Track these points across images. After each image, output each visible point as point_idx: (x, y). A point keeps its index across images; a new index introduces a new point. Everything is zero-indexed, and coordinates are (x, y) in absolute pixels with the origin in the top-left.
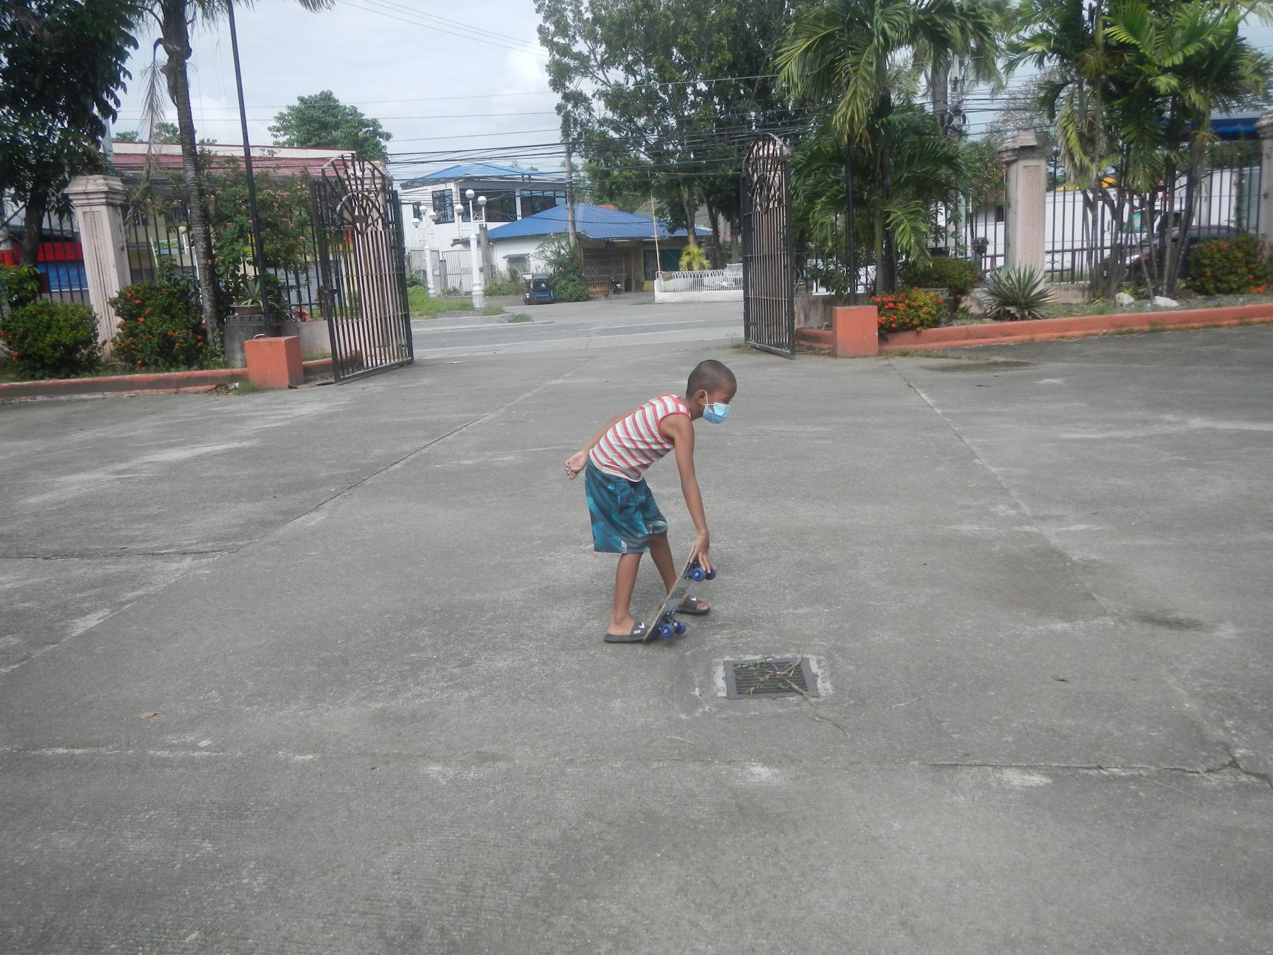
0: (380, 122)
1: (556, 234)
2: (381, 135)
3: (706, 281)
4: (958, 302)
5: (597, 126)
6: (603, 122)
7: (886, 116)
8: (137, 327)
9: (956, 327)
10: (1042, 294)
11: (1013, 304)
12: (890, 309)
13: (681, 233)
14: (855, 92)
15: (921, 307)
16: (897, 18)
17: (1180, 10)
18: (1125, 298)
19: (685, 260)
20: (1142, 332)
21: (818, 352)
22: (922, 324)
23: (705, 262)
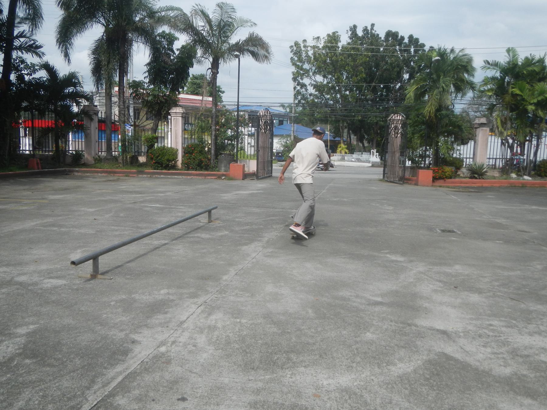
0: (221, 87)
1: (286, 135)
2: (221, 92)
3: (346, 158)
4: (457, 172)
5: (309, 96)
6: (311, 95)
7: (441, 112)
8: (191, 156)
9: (457, 180)
10: (486, 172)
11: (476, 174)
12: (436, 172)
13: (337, 139)
14: (431, 104)
15: (446, 172)
16: (447, 83)
17: (537, 85)
18: (514, 175)
19: (339, 149)
20: (518, 186)
21: (410, 184)
22: (446, 178)
23: (347, 151)
